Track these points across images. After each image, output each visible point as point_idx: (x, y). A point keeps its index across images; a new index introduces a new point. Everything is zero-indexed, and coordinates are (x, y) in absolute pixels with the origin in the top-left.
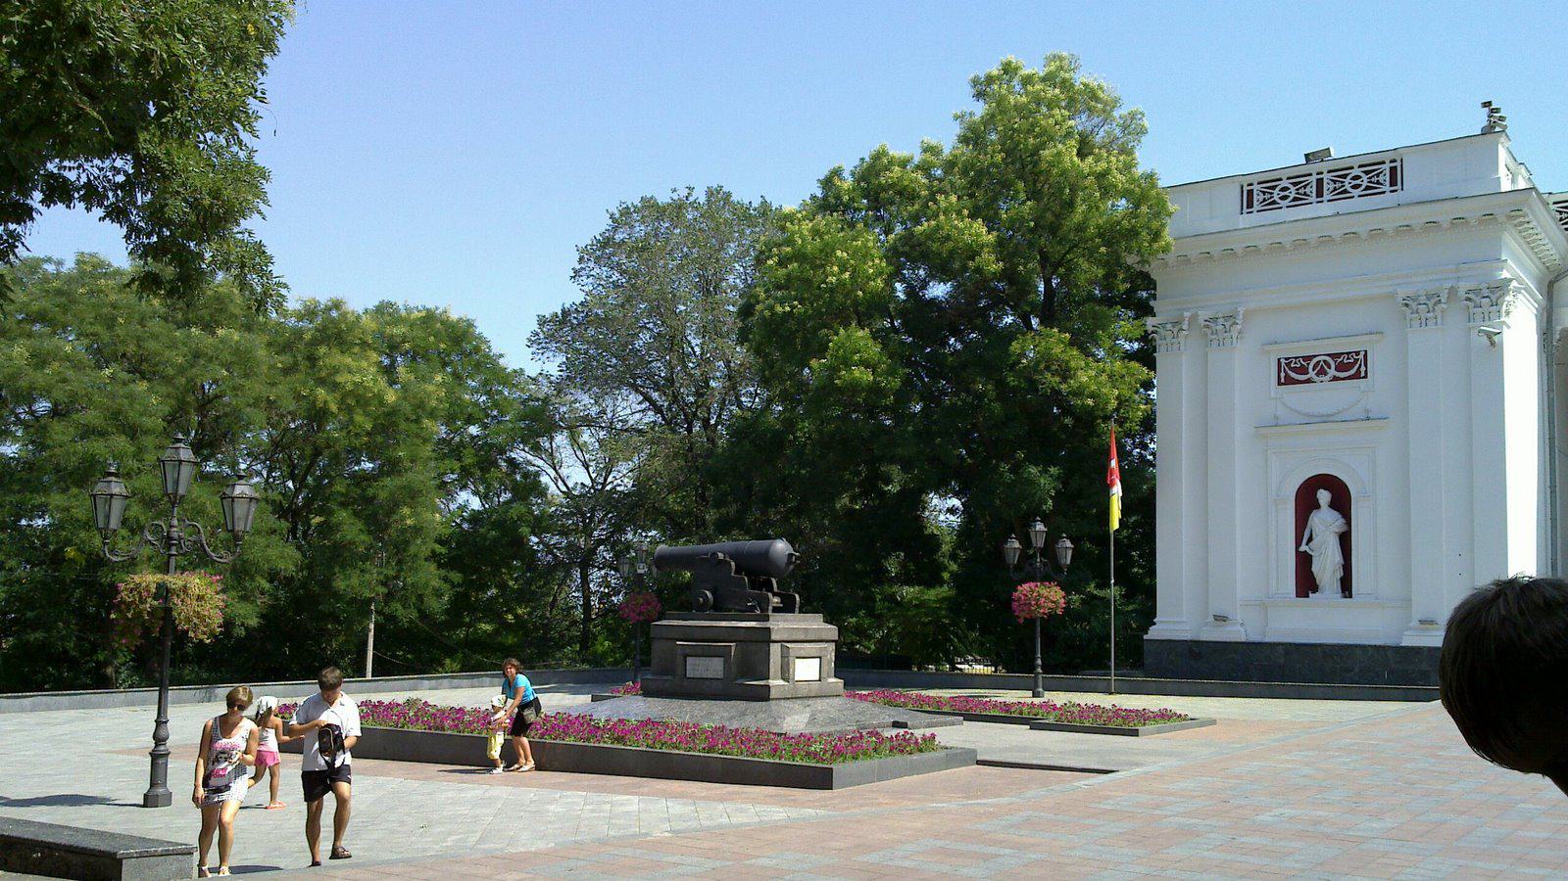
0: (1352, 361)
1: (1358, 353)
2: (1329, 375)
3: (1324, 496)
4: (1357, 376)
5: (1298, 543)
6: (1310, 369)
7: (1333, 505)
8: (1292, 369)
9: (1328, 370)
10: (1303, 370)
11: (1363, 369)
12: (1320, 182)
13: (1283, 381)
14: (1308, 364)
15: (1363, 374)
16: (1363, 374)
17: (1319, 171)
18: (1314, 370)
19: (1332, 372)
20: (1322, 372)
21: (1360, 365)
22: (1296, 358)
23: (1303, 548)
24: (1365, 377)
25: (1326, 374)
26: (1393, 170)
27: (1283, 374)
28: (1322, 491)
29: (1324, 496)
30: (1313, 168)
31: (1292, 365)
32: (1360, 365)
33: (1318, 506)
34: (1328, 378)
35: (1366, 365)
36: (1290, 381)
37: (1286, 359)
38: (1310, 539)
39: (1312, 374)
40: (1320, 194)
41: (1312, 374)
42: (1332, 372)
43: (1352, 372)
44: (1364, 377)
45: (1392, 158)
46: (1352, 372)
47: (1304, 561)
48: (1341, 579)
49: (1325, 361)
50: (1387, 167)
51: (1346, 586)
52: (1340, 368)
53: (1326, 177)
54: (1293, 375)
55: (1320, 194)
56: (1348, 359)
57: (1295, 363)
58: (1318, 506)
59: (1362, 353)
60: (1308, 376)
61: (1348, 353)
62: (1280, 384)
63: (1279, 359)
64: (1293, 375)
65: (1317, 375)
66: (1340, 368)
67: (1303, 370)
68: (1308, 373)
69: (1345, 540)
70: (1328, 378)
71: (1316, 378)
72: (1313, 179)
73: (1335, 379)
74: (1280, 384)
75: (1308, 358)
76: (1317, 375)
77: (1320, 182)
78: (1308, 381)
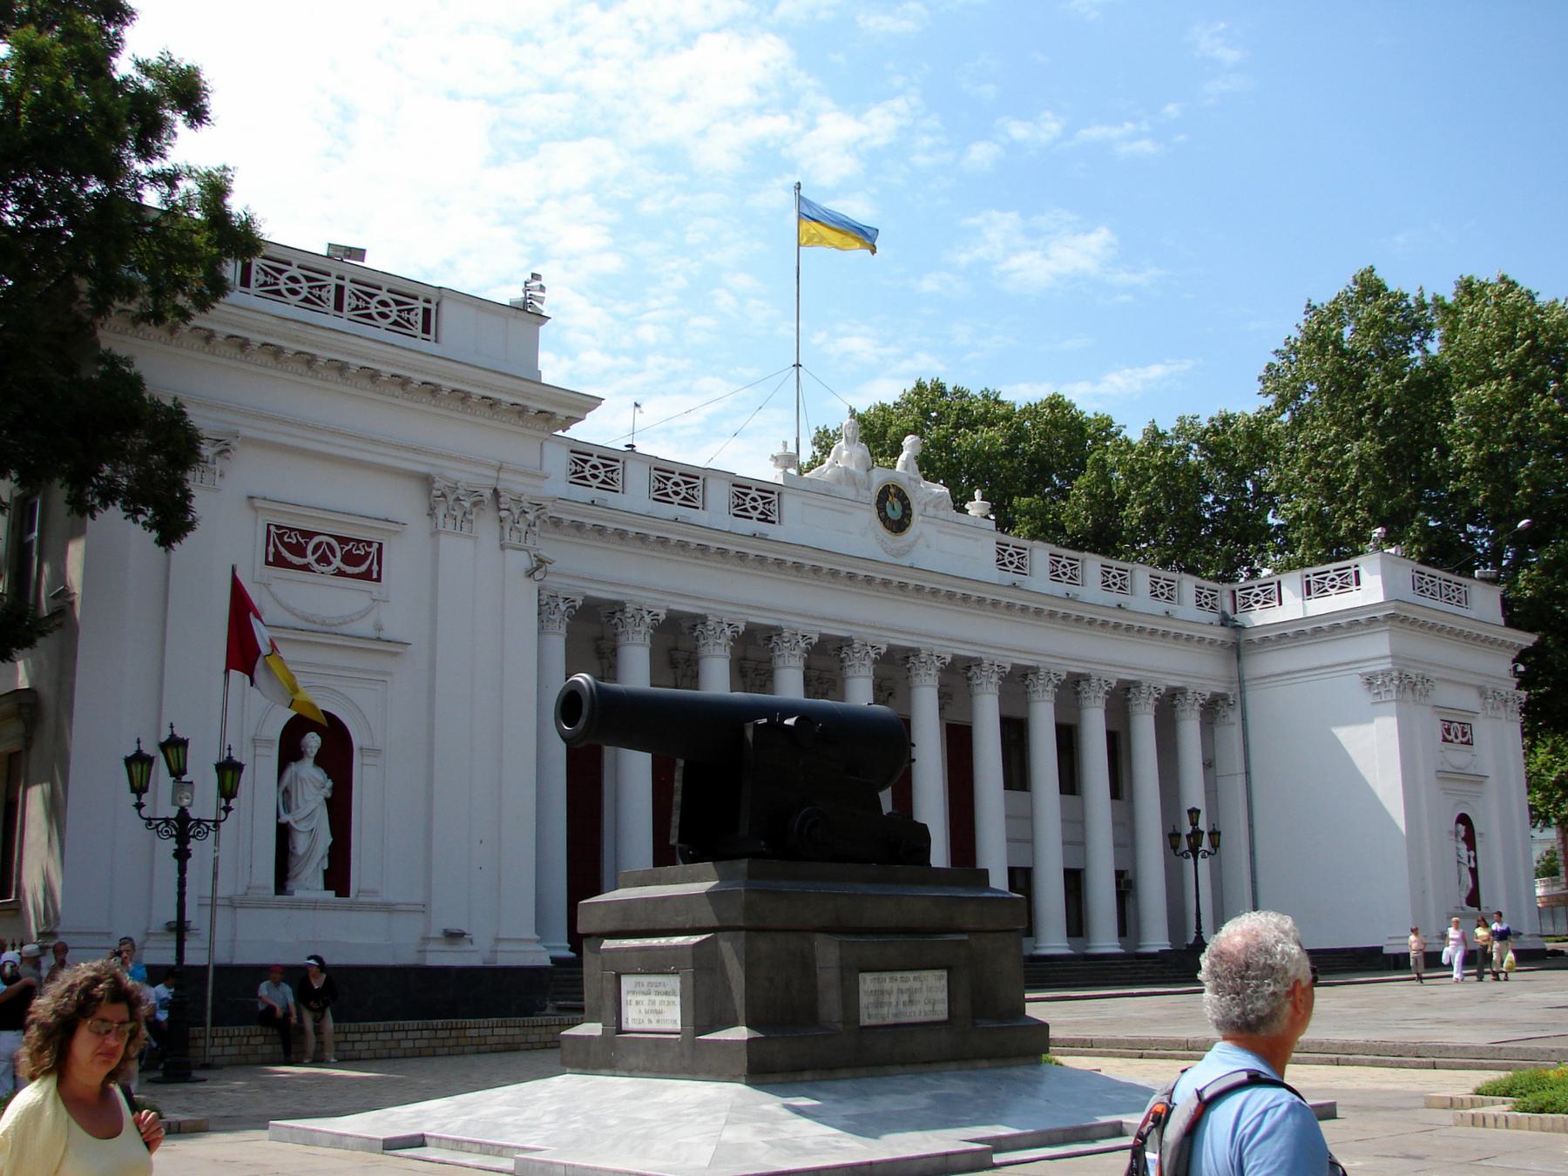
0: (363, 553)
1: (370, 544)
2: (333, 567)
3: (313, 741)
4: (366, 576)
5: (278, 816)
6: (309, 551)
7: (319, 761)
8: (288, 546)
10: (299, 550)
11: (375, 567)
12: (340, 290)
13: (271, 559)
14: (307, 543)
15: (375, 576)
16: (375, 576)
17: (341, 273)
18: (313, 554)
19: (337, 562)
20: (324, 560)
22: (292, 530)
23: (285, 818)
24: (379, 580)
25: (329, 563)
26: (427, 312)
27: (271, 549)
28: (313, 734)
29: (313, 741)
31: (286, 540)
34: (333, 567)
36: (279, 562)
37: (278, 527)
38: (288, 810)
39: (311, 559)
40: (339, 306)
41: (311, 559)
42: (337, 562)
43: (363, 568)
45: (429, 297)
46: (363, 568)
47: (284, 834)
48: (326, 872)
49: (329, 545)
50: (419, 305)
51: (338, 877)
52: (349, 559)
53: (349, 287)
54: (286, 554)
55: (339, 306)
56: (358, 549)
57: (289, 537)
59: (376, 546)
61: (359, 541)
62: (268, 563)
63: (269, 525)
64: (286, 554)
65: (317, 561)
66: (349, 559)
67: (299, 550)
68: (305, 557)
69: (339, 808)
71: (316, 566)
72: (332, 281)
73: (340, 573)
74: (268, 563)
75: (309, 535)
76: (317, 561)
77: (340, 290)
78: (306, 568)
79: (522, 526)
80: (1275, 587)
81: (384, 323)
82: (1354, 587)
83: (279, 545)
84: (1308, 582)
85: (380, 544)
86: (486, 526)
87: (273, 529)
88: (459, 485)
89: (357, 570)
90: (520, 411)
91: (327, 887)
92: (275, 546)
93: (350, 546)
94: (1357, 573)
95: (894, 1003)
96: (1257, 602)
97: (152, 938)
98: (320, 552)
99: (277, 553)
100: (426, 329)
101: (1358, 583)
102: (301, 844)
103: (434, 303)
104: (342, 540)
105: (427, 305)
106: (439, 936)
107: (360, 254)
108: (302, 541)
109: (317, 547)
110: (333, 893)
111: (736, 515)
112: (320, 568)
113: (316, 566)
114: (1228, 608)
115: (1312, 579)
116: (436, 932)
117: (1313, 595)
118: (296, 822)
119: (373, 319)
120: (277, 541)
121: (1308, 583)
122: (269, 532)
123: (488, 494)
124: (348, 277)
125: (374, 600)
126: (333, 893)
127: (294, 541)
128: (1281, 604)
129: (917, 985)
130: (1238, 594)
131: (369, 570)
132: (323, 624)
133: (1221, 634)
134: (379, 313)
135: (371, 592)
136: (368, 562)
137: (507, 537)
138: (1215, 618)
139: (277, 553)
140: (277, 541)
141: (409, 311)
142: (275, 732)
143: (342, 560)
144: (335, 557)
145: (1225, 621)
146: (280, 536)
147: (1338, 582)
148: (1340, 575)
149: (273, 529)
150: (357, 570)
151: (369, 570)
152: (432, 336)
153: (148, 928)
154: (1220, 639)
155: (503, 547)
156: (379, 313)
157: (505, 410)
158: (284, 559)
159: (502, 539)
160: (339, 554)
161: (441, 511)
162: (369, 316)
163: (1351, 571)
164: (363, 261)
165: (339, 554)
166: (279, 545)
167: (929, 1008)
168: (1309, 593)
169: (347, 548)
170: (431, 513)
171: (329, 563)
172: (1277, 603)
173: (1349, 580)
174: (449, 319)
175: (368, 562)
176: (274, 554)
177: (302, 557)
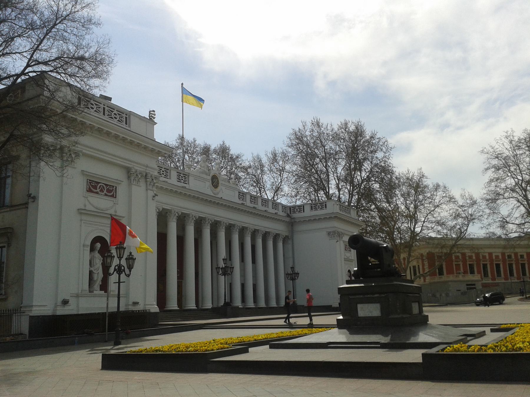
2: (104, 193)
3: (98, 245)
4: (112, 196)
6: (98, 188)
8: (92, 186)
11: (115, 193)
12: (104, 109)
13: (88, 190)
14: (97, 185)
15: (115, 196)
16: (115, 196)
17: (105, 104)
18: (99, 189)
19: (105, 192)
20: (102, 191)
21: (114, 193)
23: (92, 269)
26: (126, 118)
27: (88, 186)
28: (99, 243)
30: (104, 101)
31: (92, 184)
32: (114, 193)
34: (104, 193)
35: (116, 193)
36: (89, 191)
39: (98, 190)
40: (104, 114)
41: (98, 190)
42: (105, 192)
44: (115, 197)
46: (112, 194)
47: (91, 273)
49: (103, 186)
50: (124, 116)
53: (106, 108)
54: (92, 189)
55: (104, 114)
57: (93, 183)
59: (115, 187)
60: (96, 191)
62: (87, 191)
64: (92, 189)
65: (100, 191)
66: (109, 191)
67: (95, 188)
73: (106, 195)
76: (100, 191)
77: (104, 109)
78: (97, 193)
79: (152, 184)
80: (302, 207)
81: (116, 120)
82: (325, 208)
83: (90, 187)
84: (312, 207)
85: (116, 187)
86: (142, 183)
88: (137, 171)
89: (110, 194)
90: (152, 150)
91: (101, 290)
92: (89, 186)
94: (326, 205)
96: (297, 211)
97: (58, 307)
99: (90, 188)
100: (126, 124)
101: (326, 207)
102: (95, 277)
103: (128, 115)
104: (107, 185)
105: (126, 116)
106: (131, 304)
107: (110, 99)
109: (101, 186)
110: (103, 292)
111: (178, 181)
114: (289, 212)
115: (313, 205)
116: (131, 303)
117: (313, 210)
118: (94, 270)
119: (113, 119)
121: (312, 207)
122: (87, 181)
123: (145, 174)
124: (106, 105)
125: (114, 203)
126: (103, 292)
127: (94, 185)
128: (304, 212)
130: (292, 209)
131: (113, 195)
132: (102, 210)
133: (288, 219)
134: (114, 117)
135: (114, 201)
136: (113, 192)
137: (148, 187)
138: (285, 215)
141: (122, 117)
142: (89, 242)
143: (106, 191)
144: (104, 190)
145: (288, 216)
146: (90, 183)
147: (320, 207)
148: (321, 205)
149: (88, 180)
150: (110, 194)
151: (113, 195)
152: (128, 125)
153: (56, 304)
154: (288, 221)
155: (147, 190)
156: (114, 117)
157: (143, 147)
158: (91, 190)
159: (147, 187)
160: (105, 189)
161: (132, 178)
162: (112, 118)
163: (324, 204)
164: (111, 101)
165: (105, 189)
166: (90, 187)
168: (312, 209)
169: (108, 188)
170: (129, 178)
171: (103, 192)
172: (303, 211)
173: (323, 206)
174: (133, 120)
175: (113, 192)
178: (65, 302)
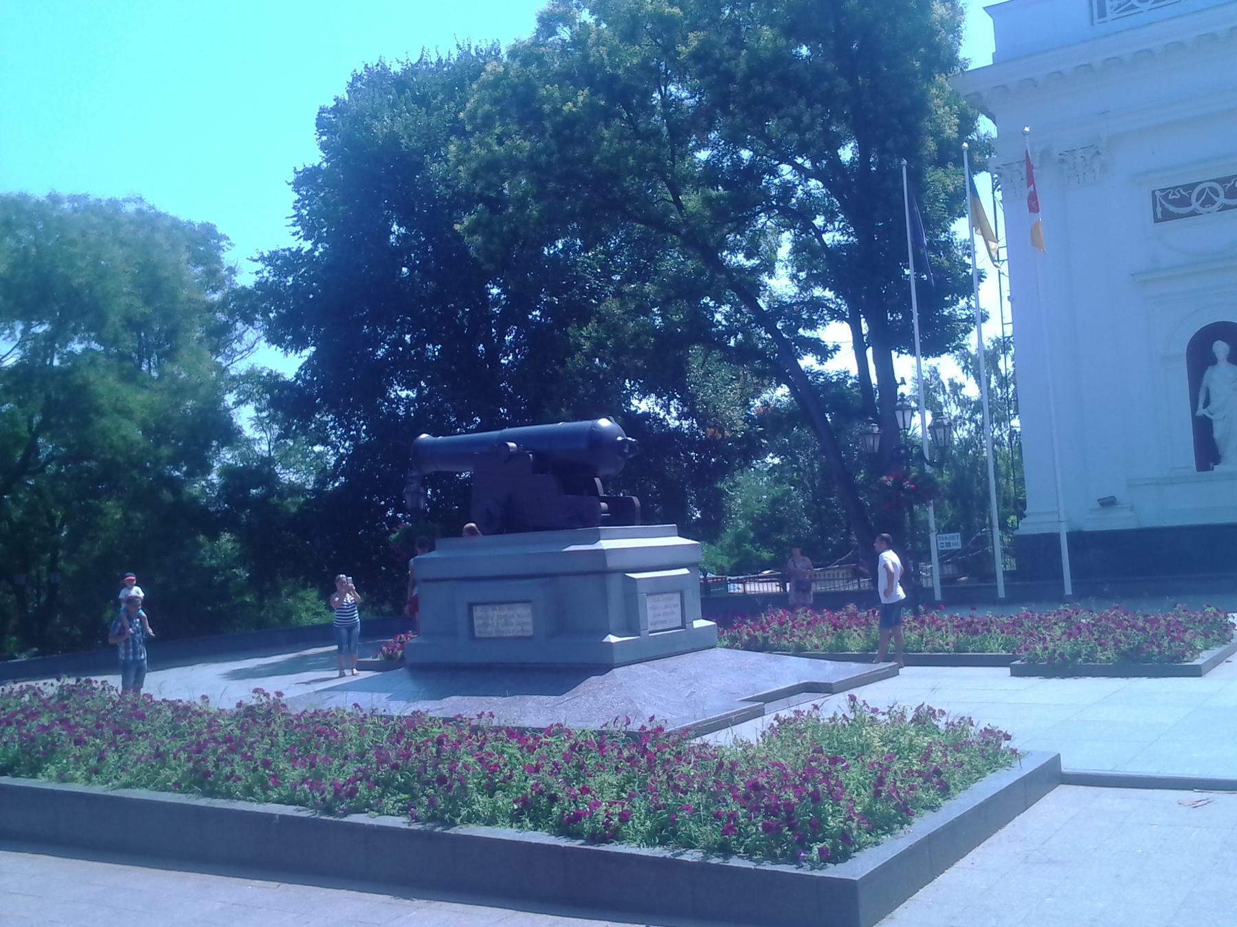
2: (1218, 204)
3: (1221, 348)
8: (1174, 202)
9: (1215, 198)
13: (1159, 216)
14: (1190, 194)
18: (1197, 200)
19: (1221, 200)
20: (1209, 201)
23: (1201, 411)
25: (1213, 203)
27: (1159, 209)
28: (1219, 342)
29: (1221, 348)
33: (1213, 361)
34: (1218, 204)
36: (1168, 216)
37: (1162, 190)
38: (1207, 403)
39: (1195, 205)
41: (1195, 205)
42: (1221, 200)
49: (1211, 189)
54: (1172, 208)
57: (1174, 194)
58: (1213, 361)
62: (1157, 220)
63: (1153, 192)
64: (1172, 208)
70: (1216, 207)
71: (1201, 210)
73: (1225, 208)
74: (1157, 220)
75: (1190, 187)
76: (1202, 205)
78: (1193, 214)
87: (1157, 193)
92: (1162, 205)
93: (1232, 183)
95: (495, 624)
98: (1203, 197)
99: (1165, 210)
104: (1221, 181)
108: (1183, 193)
112: (1204, 209)
113: (1201, 210)
120: (1163, 201)
122: (1154, 197)
129: (510, 613)
139: (1165, 210)
140: (1163, 201)
167: (520, 628)
176: (1162, 212)
177: (1213, 204)
178: (1108, 503)
